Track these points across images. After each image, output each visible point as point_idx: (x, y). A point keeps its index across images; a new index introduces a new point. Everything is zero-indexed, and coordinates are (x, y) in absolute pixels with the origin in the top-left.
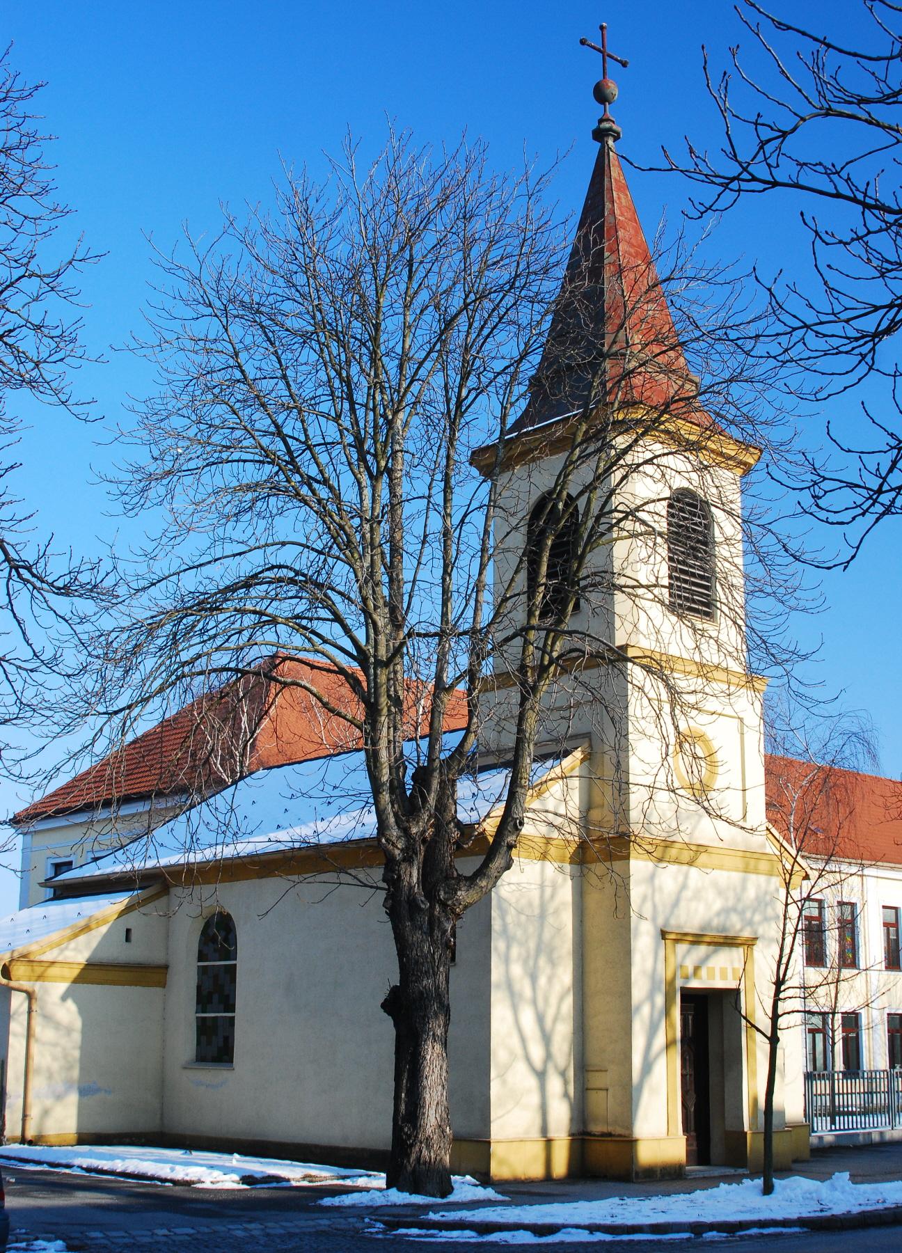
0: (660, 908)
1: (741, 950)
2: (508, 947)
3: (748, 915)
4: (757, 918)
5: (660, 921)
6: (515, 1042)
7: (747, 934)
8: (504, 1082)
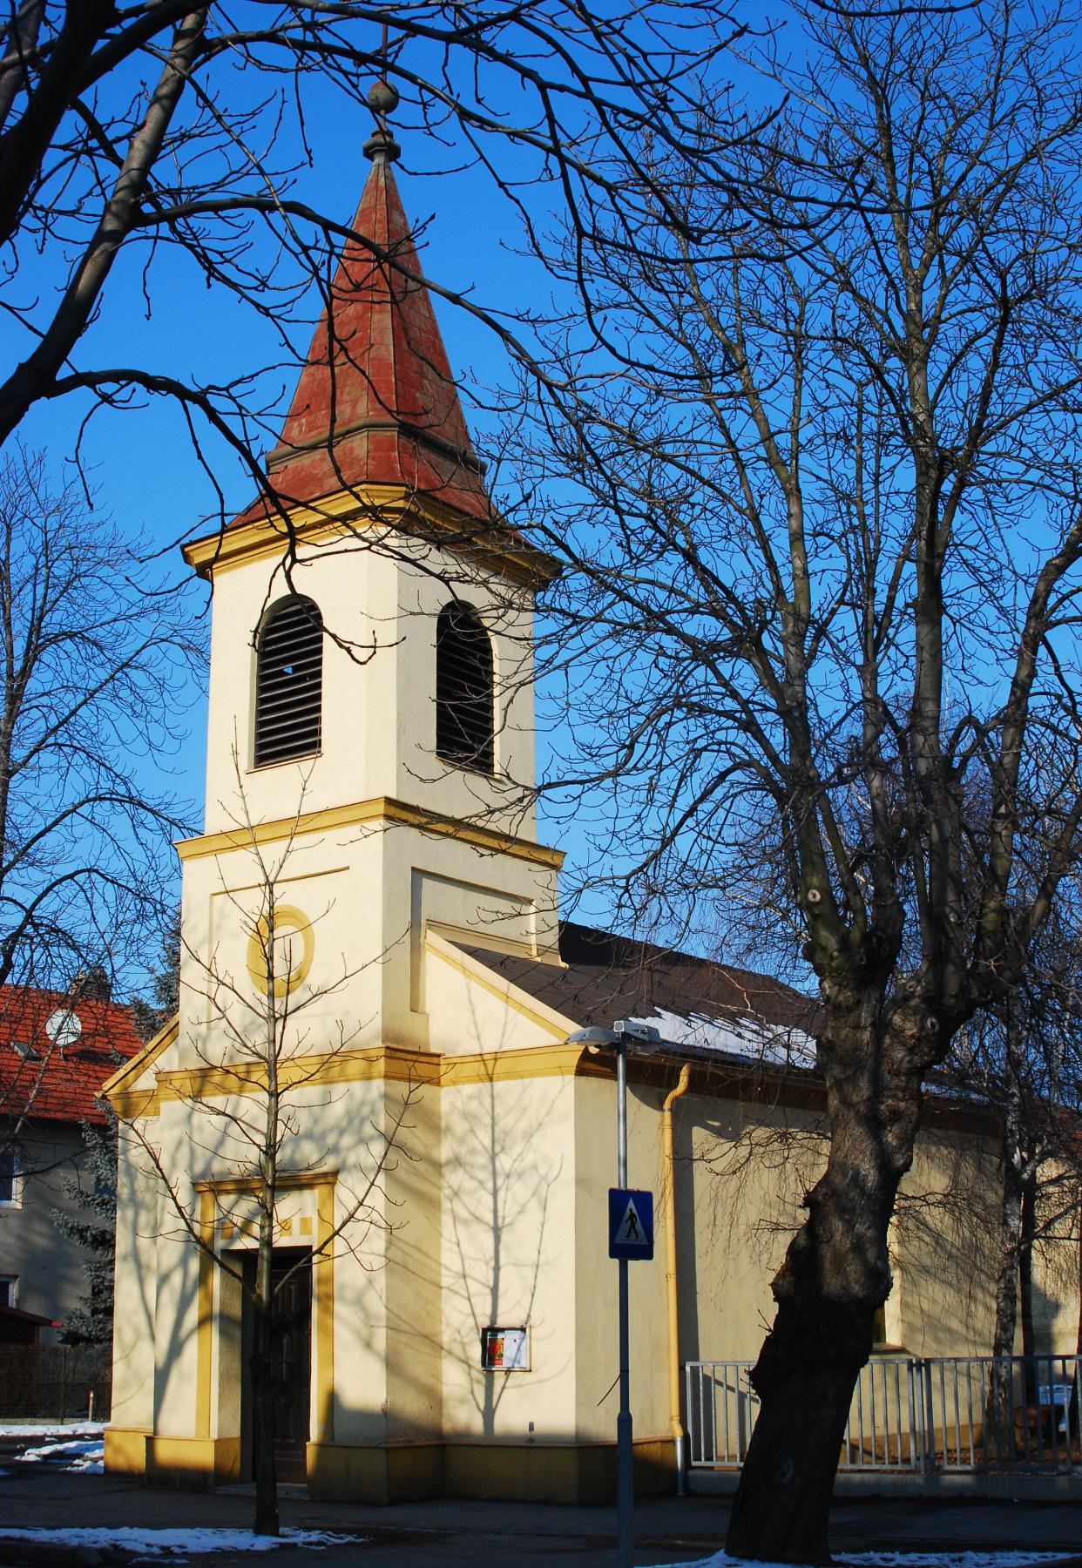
0: (199, 1151)
1: (316, 1191)
2: (136, 1215)
3: (331, 1140)
4: (347, 1141)
5: (199, 1167)
6: (141, 1320)
7: (329, 1164)
8: (129, 1365)
